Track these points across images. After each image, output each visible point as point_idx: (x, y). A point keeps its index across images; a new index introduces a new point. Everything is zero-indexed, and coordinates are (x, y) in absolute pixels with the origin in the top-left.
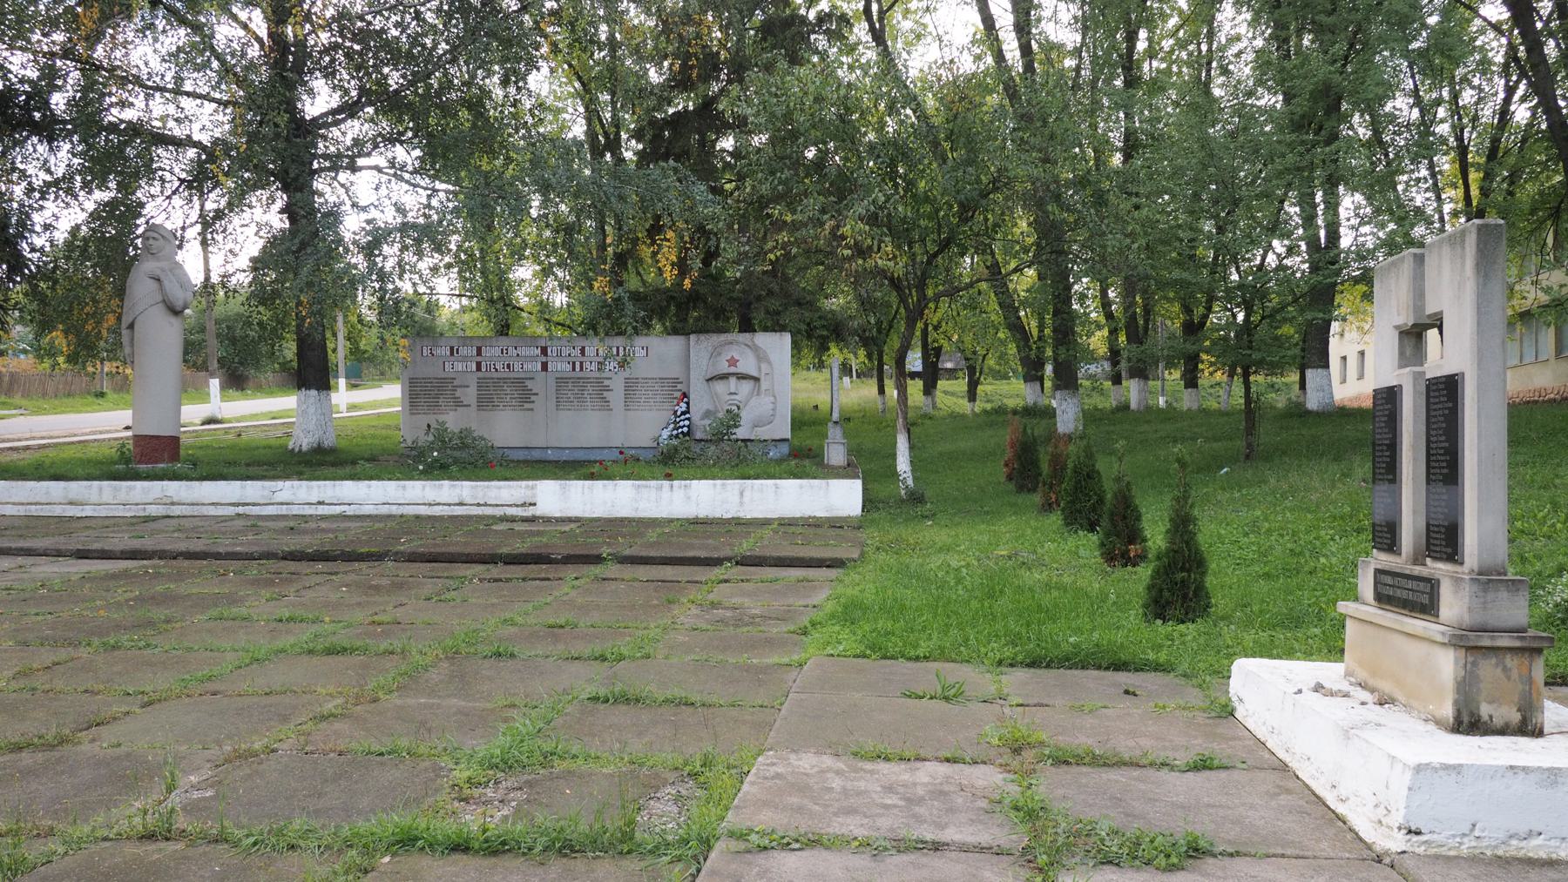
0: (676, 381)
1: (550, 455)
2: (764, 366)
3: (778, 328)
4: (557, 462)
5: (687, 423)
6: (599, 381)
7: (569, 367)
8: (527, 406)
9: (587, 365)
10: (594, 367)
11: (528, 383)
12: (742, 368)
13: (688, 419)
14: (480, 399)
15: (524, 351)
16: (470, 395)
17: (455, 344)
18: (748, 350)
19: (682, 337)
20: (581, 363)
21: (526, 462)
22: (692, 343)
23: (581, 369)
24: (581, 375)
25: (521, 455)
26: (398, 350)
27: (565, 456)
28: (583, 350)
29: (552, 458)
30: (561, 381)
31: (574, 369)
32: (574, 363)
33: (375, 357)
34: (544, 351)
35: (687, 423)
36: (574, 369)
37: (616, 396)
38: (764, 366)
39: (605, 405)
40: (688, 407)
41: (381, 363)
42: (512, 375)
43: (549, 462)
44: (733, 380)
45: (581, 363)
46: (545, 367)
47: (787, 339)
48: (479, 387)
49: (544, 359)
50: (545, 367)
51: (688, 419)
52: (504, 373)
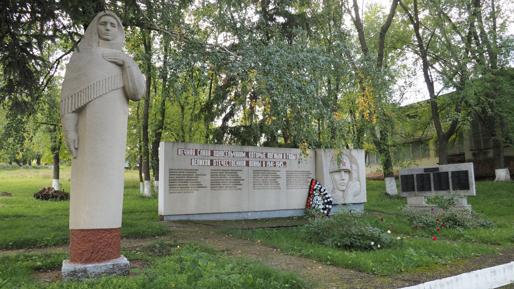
6: (274, 172)
7: (260, 164)
10: (272, 164)
11: (239, 173)
14: (212, 183)
16: (206, 180)
20: (266, 162)
23: (266, 166)
24: (265, 169)
28: (266, 155)
30: (256, 172)
31: (262, 166)
32: (262, 162)
36: (262, 166)
37: (282, 181)
39: (277, 186)
45: (266, 162)
49: (247, 159)
52: (226, 167)
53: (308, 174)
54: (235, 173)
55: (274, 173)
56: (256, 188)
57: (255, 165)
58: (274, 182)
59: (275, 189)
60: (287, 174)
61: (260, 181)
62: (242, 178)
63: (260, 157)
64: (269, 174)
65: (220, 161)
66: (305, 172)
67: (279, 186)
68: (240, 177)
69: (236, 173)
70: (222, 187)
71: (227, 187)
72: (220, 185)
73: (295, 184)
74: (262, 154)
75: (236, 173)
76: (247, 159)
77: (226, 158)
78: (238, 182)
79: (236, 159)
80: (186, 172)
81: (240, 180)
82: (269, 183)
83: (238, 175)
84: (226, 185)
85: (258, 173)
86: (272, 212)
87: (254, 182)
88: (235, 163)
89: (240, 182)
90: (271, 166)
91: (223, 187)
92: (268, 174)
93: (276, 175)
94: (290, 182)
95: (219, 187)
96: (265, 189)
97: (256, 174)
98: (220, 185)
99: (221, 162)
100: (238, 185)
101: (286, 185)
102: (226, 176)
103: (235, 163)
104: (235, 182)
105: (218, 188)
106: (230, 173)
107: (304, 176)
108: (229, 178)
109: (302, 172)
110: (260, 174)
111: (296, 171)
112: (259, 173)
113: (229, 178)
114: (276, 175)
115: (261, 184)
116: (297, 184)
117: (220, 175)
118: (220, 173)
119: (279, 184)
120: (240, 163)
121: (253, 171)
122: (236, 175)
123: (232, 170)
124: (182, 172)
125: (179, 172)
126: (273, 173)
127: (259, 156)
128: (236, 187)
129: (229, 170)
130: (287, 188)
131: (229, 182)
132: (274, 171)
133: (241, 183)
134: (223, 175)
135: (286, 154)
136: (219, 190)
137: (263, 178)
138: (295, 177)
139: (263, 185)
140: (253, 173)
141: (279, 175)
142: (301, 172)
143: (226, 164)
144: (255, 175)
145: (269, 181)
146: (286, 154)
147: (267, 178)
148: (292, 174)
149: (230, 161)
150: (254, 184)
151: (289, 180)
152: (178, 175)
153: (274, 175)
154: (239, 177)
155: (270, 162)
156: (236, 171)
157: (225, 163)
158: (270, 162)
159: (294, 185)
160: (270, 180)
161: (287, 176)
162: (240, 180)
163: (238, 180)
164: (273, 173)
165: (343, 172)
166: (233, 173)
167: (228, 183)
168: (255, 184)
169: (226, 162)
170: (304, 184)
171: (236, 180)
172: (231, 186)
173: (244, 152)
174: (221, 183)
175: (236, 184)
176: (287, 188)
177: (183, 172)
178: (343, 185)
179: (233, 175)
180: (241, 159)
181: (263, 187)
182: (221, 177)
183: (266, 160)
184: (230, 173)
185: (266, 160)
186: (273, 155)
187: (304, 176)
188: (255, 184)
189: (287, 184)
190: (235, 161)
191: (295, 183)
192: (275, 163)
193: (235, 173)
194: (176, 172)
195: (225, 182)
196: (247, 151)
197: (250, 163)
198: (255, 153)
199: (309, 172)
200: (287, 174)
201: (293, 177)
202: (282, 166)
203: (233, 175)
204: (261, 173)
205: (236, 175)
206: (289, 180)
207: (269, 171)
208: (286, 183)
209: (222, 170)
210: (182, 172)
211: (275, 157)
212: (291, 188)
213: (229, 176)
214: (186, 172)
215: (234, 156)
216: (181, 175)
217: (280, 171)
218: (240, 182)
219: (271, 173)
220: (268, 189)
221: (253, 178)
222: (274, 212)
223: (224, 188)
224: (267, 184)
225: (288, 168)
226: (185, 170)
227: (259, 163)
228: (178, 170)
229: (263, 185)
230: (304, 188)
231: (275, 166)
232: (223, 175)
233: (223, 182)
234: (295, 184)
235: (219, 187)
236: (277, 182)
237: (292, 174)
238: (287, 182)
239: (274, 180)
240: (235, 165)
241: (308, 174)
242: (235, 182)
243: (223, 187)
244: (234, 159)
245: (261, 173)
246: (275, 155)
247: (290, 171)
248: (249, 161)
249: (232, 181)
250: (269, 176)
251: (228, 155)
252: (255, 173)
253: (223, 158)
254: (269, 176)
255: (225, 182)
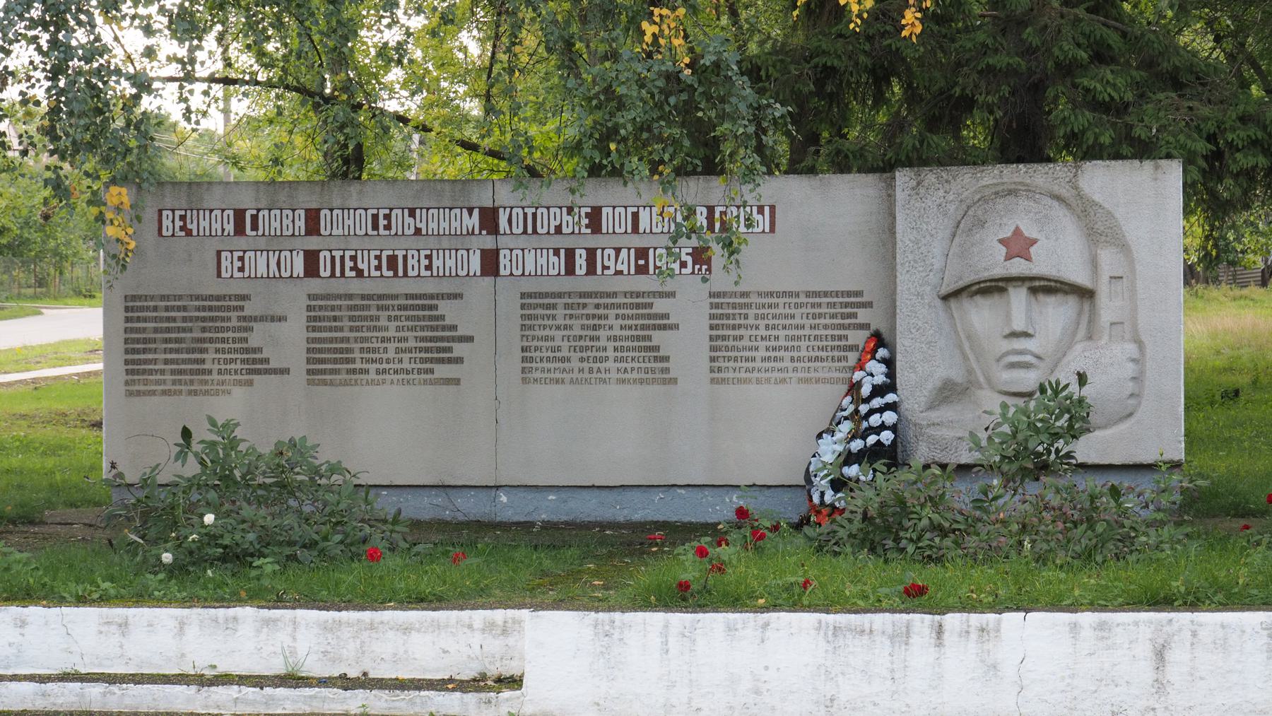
0: (853, 300)
1: (506, 507)
2: (1109, 259)
3: (1143, 150)
4: (526, 526)
5: (890, 417)
6: (640, 301)
7: (558, 264)
8: (442, 371)
9: (606, 258)
10: (626, 262)
11: (444, 307)
12: (1042, 263)
13: (892, 407)
15: (433, 222)
17: (247, 201)
18: (1058, 211)
19: (871, 179)
20: (591, 253)
21: (441, 525)
22: (900, 195)
23: (591, 270)
24: (590, 284)
25: (423, 507)
26: (101, 219)
27: (547, 509)
28: (595, 218)
29: (509, 515)
31: (570, 270)
32: (570, 254)
33: (25, 242)
34: (489, 220)
35: (890, 417)
36: (570, 270)
38: (1109, 259)
40: (891, 374)
41: (39, 257)
42: (402, 287)
43: (505, 526)
44: (1018, 297)
45: (591, 253)
46: (490, 263)
47: (1172, 175)
48: (313, 322)
49: (488, 242)
50: (490, 263)
51: (892, 407)
53: (847, 305)
54: (423, 308)
55: (638, 306)
56: (538, 375)
57: (530, 268)
58: (640, 349)
59: (641, 381)
60: (717, 306)
61: (558, 343)
62: (460, 332)
63: (558, 230)
64: (612, 313)
65: (348, 254)
66: (826, 294)
67: (667, 370)
68: (454, 328)
69: (431, 308)
70: (362, 371)
71: (384, 371)
72: (353, 361)
73: (764, 360)
74: (570, 210)
75: (431, 308)
76: (488, 242)
77: (378, 243)
78: (439, 350)
79: (432, 243)
80: (198, 309)
81: (453, 339)
82: (610, 353)
83: (442, 317)
84: (381, 361)
85: (549, 307)
86: (629, 494)
87: (524, 349)
88: (425, 262)
89: (450, 350)
90: (621, 273)
91: (367, 371)
92: (601, 311)
93: (650, 316)
94: (733, 348)
95: (349, 372)
96: (587, 381)
97: (540, 311)
98: (353, 361)
99: (354, 258)
100: (441, 361)
101: (706, 364)
102: (384, 322)
103: (425, 262)
104: (427, 350)
105: (344, 376)
106: (401, 308)
107: (820, 316)
108: (398, 329)
109: (808, 294)
110: (560, 312)
111: (771, 294)
112: (554, 306)
113: (398, 329)
114: (650, 316)
115: (563, 360)
116: (776, 359)
117: (351, 319)
118: (350, 308)
119: (666, 359)
120: (450, 263)
121: (523, 295)
122: (431, 318)
123: (408, 296)
124: (179, 309)
125: (167, 309)
126: (632, 306)
127: (553, 224)
128: (432, 371)
129: (396, 297)
130: (713, 381)
131: (398, 351)
132: (638, 295)
133: (455, 354)
134: (365, 318)
135: (711, 210)
136: (345, 383)
137: (577, 332)
138: (762, 323)
139: (575, 364)
140: (523, 307)
141: (666, 316)
142: (803, 299)
143: (379, 268)
144: (530, 317)
145: (611, 345)
146: (711, 210)
147: (595, 327)
148: (749, 306)
149: (400, 254)
150: (524, 360)
151: (724, 338)
152: (161, 319)
153: (638, 317)
154: (444, 328)
155: (618, 251)
156: (432, 297)
157: (374, 263)
158: (618, 251)
159: (758, 364)
160: (615, 338)
161: (712, 317)
162: (453, 339)
163: (442, 339)
164: (632, 306)
165: (1018, 297)
166: (413, 307)
167: (391, 354)
168: (531, 360)
169: (378, 258)
170: (817, 359)
171: (431, 339)
172: (406, 365)
173: (470, 211)
174: (357, 355)
175: (431, 360)
176: (713, 381)
177: (185, 309)
178: (1013, 366)
179: (418, 318)
180: (456, 243)
181: (575, 375)
182: (358, 329)
183: (593, 241)
184: (401, 308)
185: (593, 241)
186: (635, 216)
187: (820, 316)
188: (531, 360)
189: (713, 359)
190: (423, 253)
191: (762, 353)
192: (642, 253)
193: (423, 308)
194: (155, 309)
195: (374, 350)
196: (489, 204)
197: (502, 261)
198: (530, 211)
199: (858, 294)
200: (717, 306)
201: (751, 321)
202: (689, 270)
203: (418, 318)
204: (567, 306)
205: (431, 318)
206: (724, 338)
207: (609, 295)
208: (707, 354)
209: (363, 297)
210: (179, 309)
211: (644, 224)
212: (740, 381)
213: (393, 324)
214: (198, 309)
215: (418, 231)
216: (174, 319)
217: (671, 295)
218: (450, 350)
219: (619, 306)
220: (604, 381)
221: (518, 333)
222: (636, 494)
223: (372, 375)
224: (595, 360)
225: (721, 279)
226: (191, 297)
227: (553, 259)
228: (163, 298)
229: (575, 364)
230: (817, 381)
231: (642, 270)
232: (365, 318)
233: (369, 350)
234: (764, 360)
235: (349, 372)
236: (657, 348)
237: (749, 306)
238: (713, 349)
239: (638, 338)
240: (424, 273)
241: (847, 305)
242: (427, 350)
243: (367, 371)
244: (420, 242)
245: (567, 306)
246: (644, 216)
247: (734, 294)
248: (497, 251)
249: (412, 344)
250: (611, 321)
251: (388, 227)
252: (530, 306)
253: (367, 243)
254: (611, 321)
255: (374, 350)
